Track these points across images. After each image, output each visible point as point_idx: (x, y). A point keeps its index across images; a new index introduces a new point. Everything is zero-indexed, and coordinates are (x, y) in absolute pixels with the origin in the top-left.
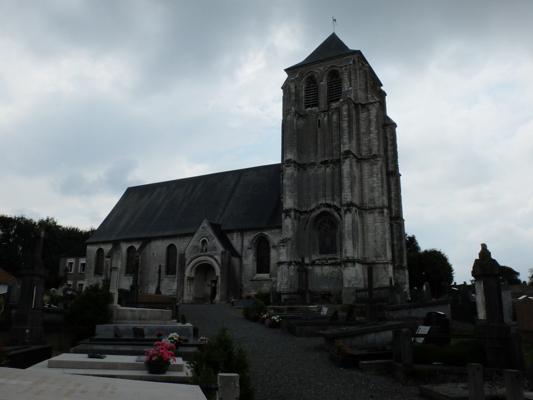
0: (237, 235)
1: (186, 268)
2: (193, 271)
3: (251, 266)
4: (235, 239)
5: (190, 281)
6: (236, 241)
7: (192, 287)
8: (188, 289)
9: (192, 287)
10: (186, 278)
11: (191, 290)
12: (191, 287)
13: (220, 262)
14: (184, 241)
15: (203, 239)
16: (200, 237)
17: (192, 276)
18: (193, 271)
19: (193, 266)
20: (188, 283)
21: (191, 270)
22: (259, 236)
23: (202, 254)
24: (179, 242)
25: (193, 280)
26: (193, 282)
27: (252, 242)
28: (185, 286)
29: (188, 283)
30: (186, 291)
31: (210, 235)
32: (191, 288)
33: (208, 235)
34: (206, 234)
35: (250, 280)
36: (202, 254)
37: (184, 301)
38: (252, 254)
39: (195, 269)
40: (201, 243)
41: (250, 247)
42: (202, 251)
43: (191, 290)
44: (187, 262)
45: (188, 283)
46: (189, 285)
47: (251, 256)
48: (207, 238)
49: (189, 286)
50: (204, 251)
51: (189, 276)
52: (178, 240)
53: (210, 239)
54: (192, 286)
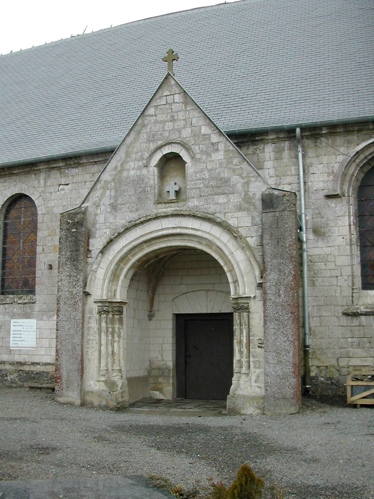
0: (279, 152)
1: (95, 266)
2: (122, 277)
3: (344, 260)
4: (269, 164)
5: (110, 316)
6: (272, 172)
7: (116, 339)
8: (102, 348)
9: (116, 339)
10: (92, 307)
11: (113, 351)
12: (113, 342)
13: (253, 241)
14: (63, 181)
15: (167, 150)
16: (153, 146)
17: (118, 299)
18: (122, 277)
19: (124, 259)
20: (100, 324)
21: (115, 276)
22: (362, 156)
23: (163, 209)
24: (45, 186)
25: (121, 312)
26: (121, 321)
27: (344, 175)
28: (92, 336)
29: (104, 324)
30: (96, 354)
31: (196, 135)
32: (116, 345)
33: (186, 133)
34: (180, 131)
35: (346, 314)
36: (163, 209)
37: (88, 398)
38: (347, 218)
39: (129, 269)
40: (156, 169)
41: (338, 192)
42: (160, 200)
43: (113, 351)
44: (96, 244)
45: (100, 324)
46: (107, 331)
47: (340, 223)
48: (183, 145)
49: (107, 336)
50: (172, 196)
51: (105, 298)
52: (42, 182)
53: (196, 149)
54: (119, 337)
